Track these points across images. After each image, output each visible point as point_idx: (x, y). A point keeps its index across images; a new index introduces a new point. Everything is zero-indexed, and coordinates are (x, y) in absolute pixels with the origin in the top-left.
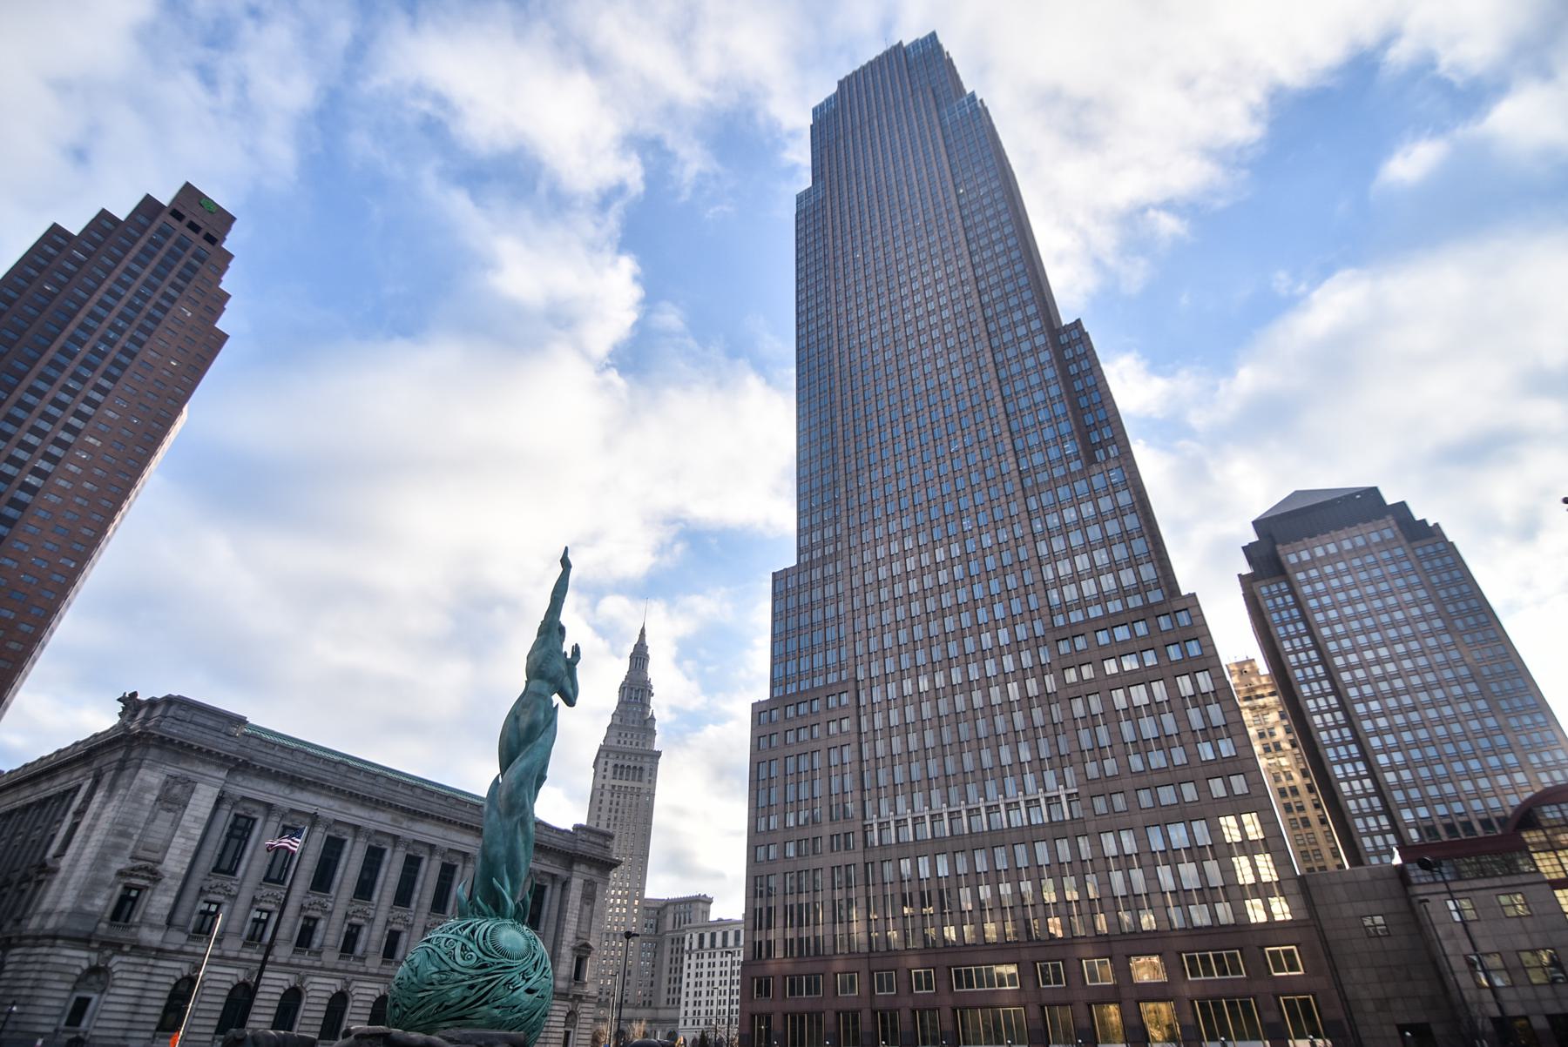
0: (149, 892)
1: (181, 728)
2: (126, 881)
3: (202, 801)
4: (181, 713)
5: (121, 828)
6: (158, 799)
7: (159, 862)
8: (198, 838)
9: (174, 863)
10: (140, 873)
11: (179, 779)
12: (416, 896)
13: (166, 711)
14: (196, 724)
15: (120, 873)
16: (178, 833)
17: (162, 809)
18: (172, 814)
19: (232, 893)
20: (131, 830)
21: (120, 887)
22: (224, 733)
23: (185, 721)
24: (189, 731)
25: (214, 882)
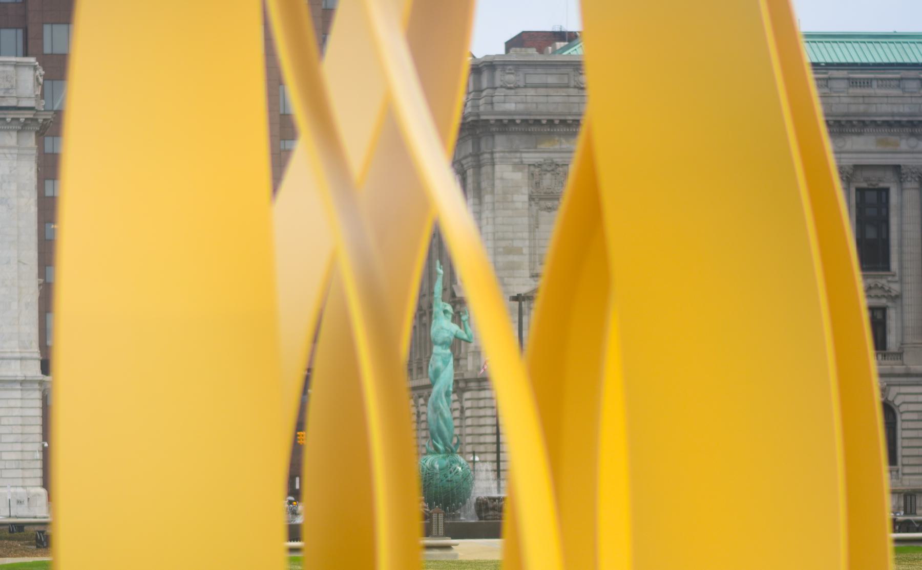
1: (518, 99)
4: (511, 78)
5: (503, 244)
6: (531, 198)
11: (545, 167)
13: (492, 78)
14: (535, 86)
17: (541, 209)
20: (517, 244)
22: (575, 87)
23: (518, 87)
24: (529, 99)
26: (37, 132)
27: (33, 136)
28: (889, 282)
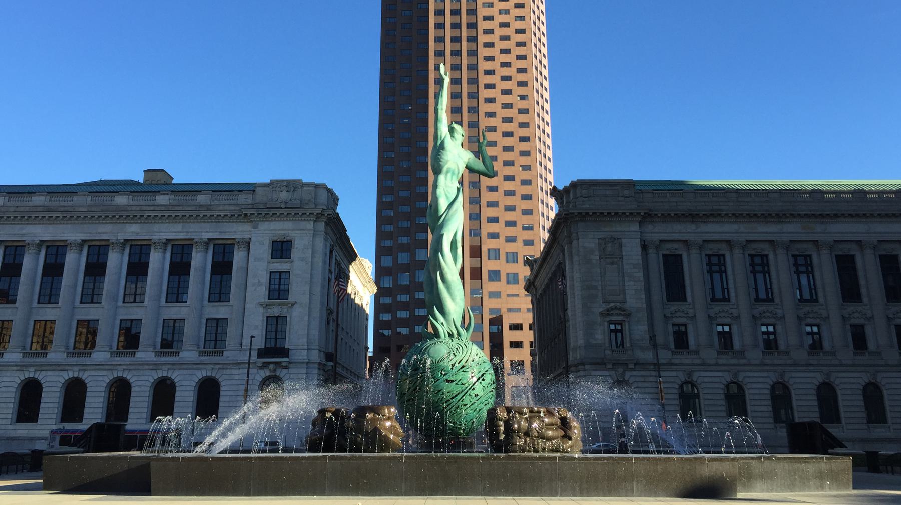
0: (627, 324)
2: (608, 320)
3: (632, 252)
7: (625, 302)
8: (642, 279)
9: (634, 300)
10: (614, 312)
12: (864, 291)
15: (602, 314)
16: (626, 279)
18: (615, 266)
19: (690, 315)
21: (606, 324)
25: (673, 309)
26: (326, 222)
27: (323, 224)
28: (820, 309)
